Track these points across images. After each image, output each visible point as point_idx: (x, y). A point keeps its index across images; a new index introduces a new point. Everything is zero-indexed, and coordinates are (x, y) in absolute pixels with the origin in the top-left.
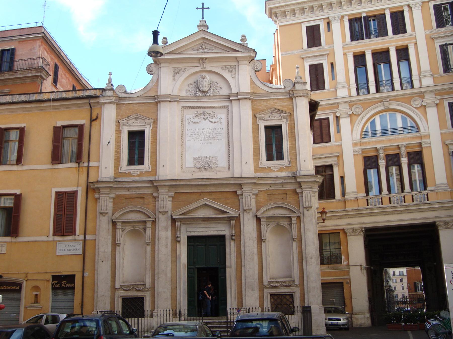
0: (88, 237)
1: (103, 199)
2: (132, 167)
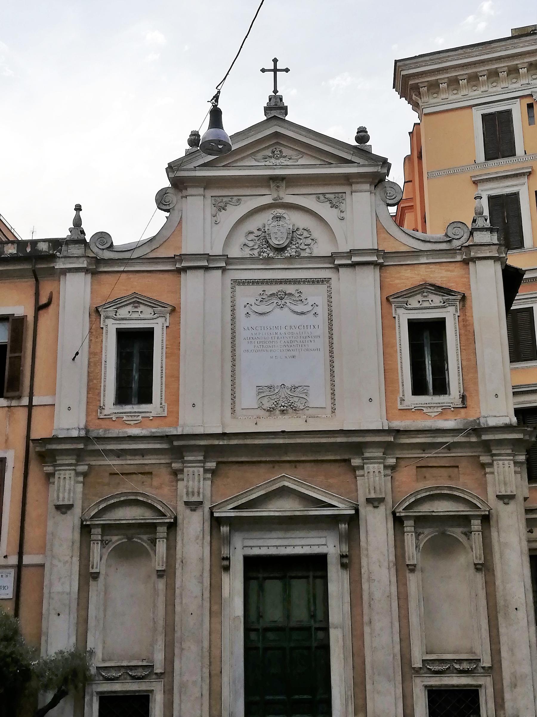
0: (27, 560)
1: (62, 477)
2: (128, 408)
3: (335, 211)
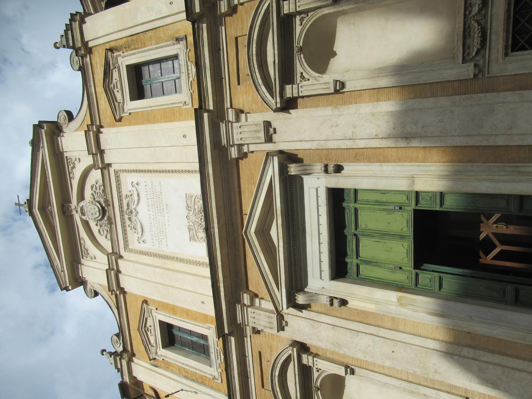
3: (77, 165)
